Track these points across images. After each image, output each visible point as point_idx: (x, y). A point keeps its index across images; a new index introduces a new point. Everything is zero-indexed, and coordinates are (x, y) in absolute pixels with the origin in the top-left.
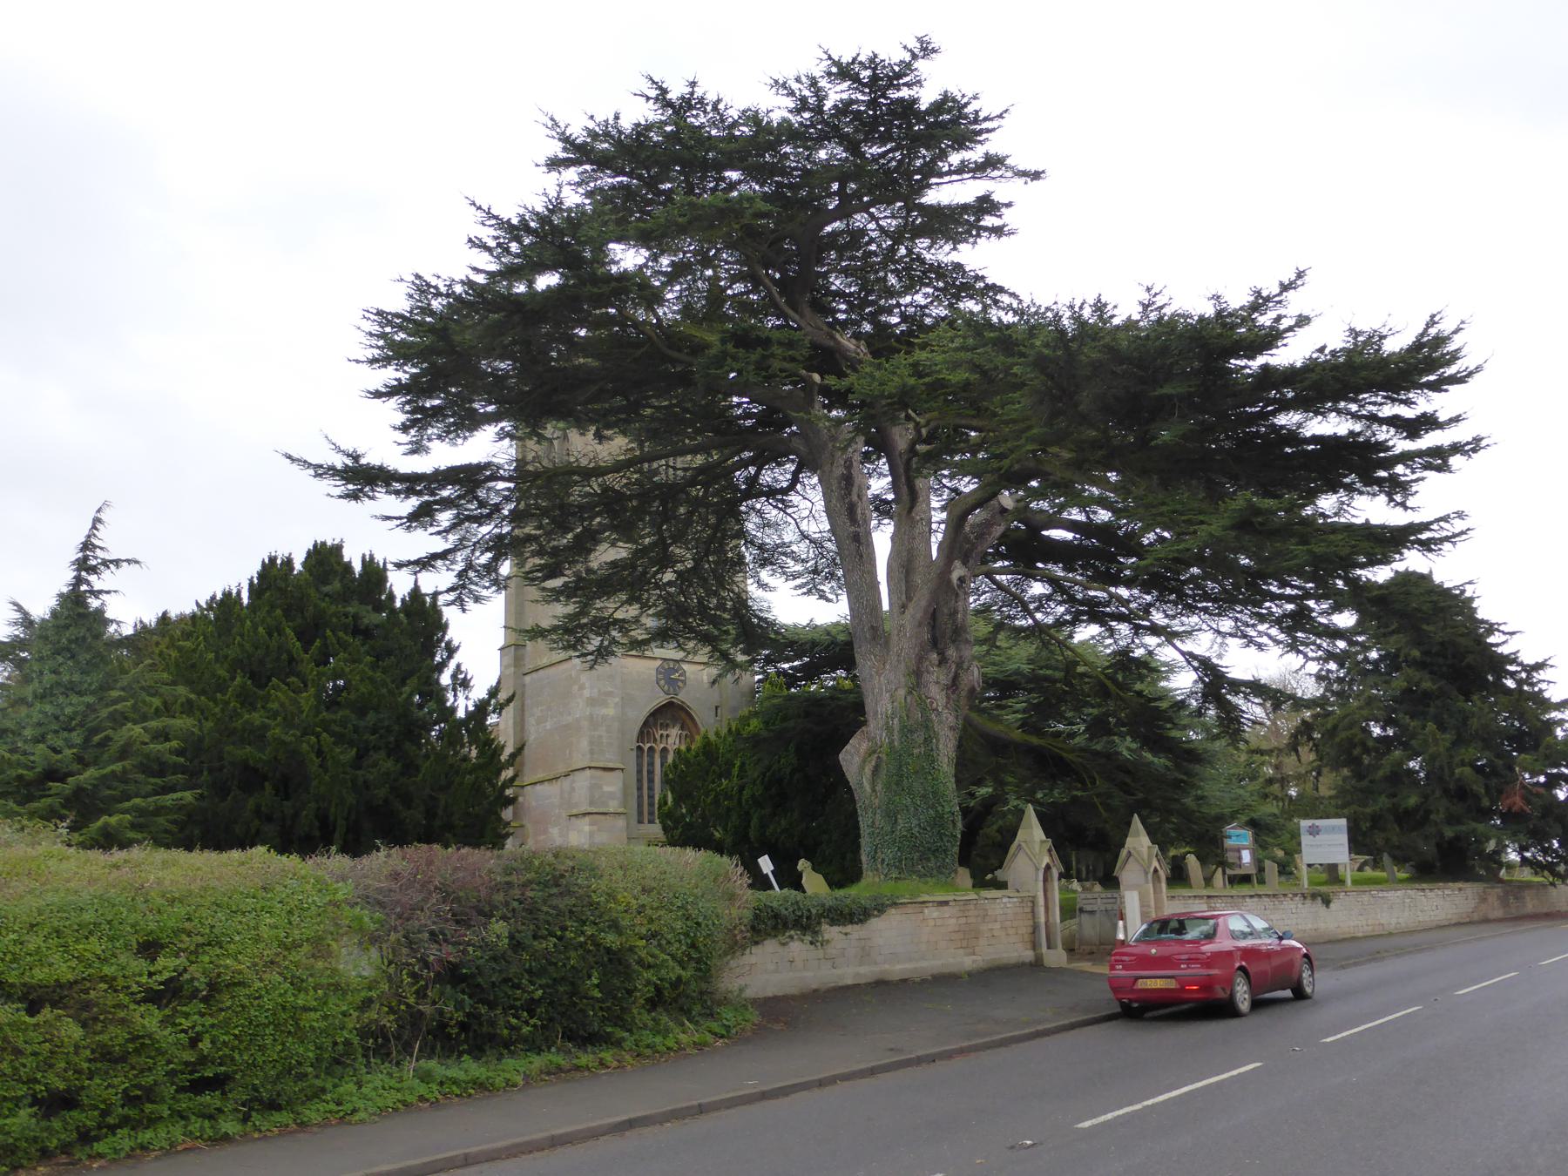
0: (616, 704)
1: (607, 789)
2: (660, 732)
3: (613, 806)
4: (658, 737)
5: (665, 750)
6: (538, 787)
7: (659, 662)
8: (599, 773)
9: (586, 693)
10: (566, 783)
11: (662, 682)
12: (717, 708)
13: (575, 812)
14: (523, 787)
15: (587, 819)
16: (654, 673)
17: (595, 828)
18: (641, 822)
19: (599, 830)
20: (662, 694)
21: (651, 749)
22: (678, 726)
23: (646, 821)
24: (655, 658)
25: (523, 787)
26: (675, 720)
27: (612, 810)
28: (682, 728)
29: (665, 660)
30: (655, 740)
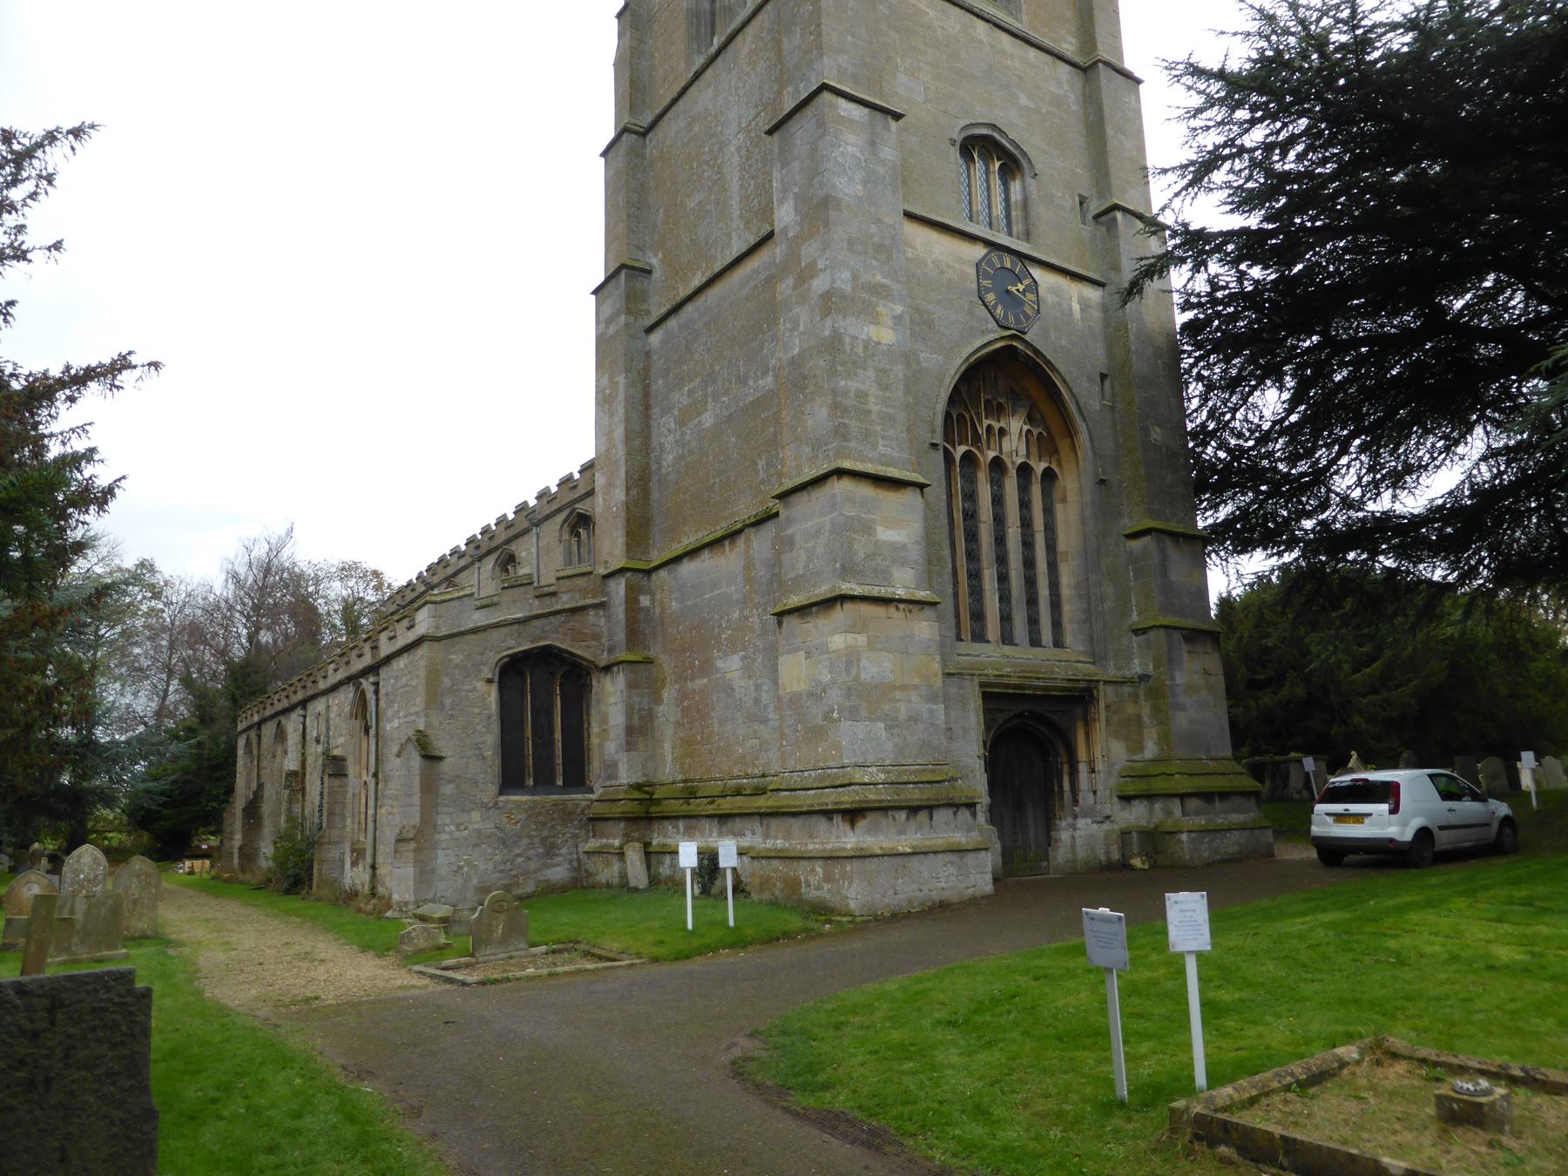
0: (898, 319)
1: (885, 535)
2: (986, 422)
3: (903, 583)
4: (982, 431)
5: (997, 465)
6: (687, 568)
7: (979, 251)
8: (865, 490)
9: (819, 284)
10: (760, 543)
11: (990, 297)
12: (1103, 377)
13: (795, 600)
14: (648, 572)
15: (840, 614)
17: (862, 639)
18: (959, 638)
19: (872, 646)
20: (992, 325)
21: (967, 456)
22: (1022, 413)
23: (966, 634)
25: (648, 572)
26: (1017, 399)
27: (901, 593)
28: (1030, 419)
30: (977, 439)
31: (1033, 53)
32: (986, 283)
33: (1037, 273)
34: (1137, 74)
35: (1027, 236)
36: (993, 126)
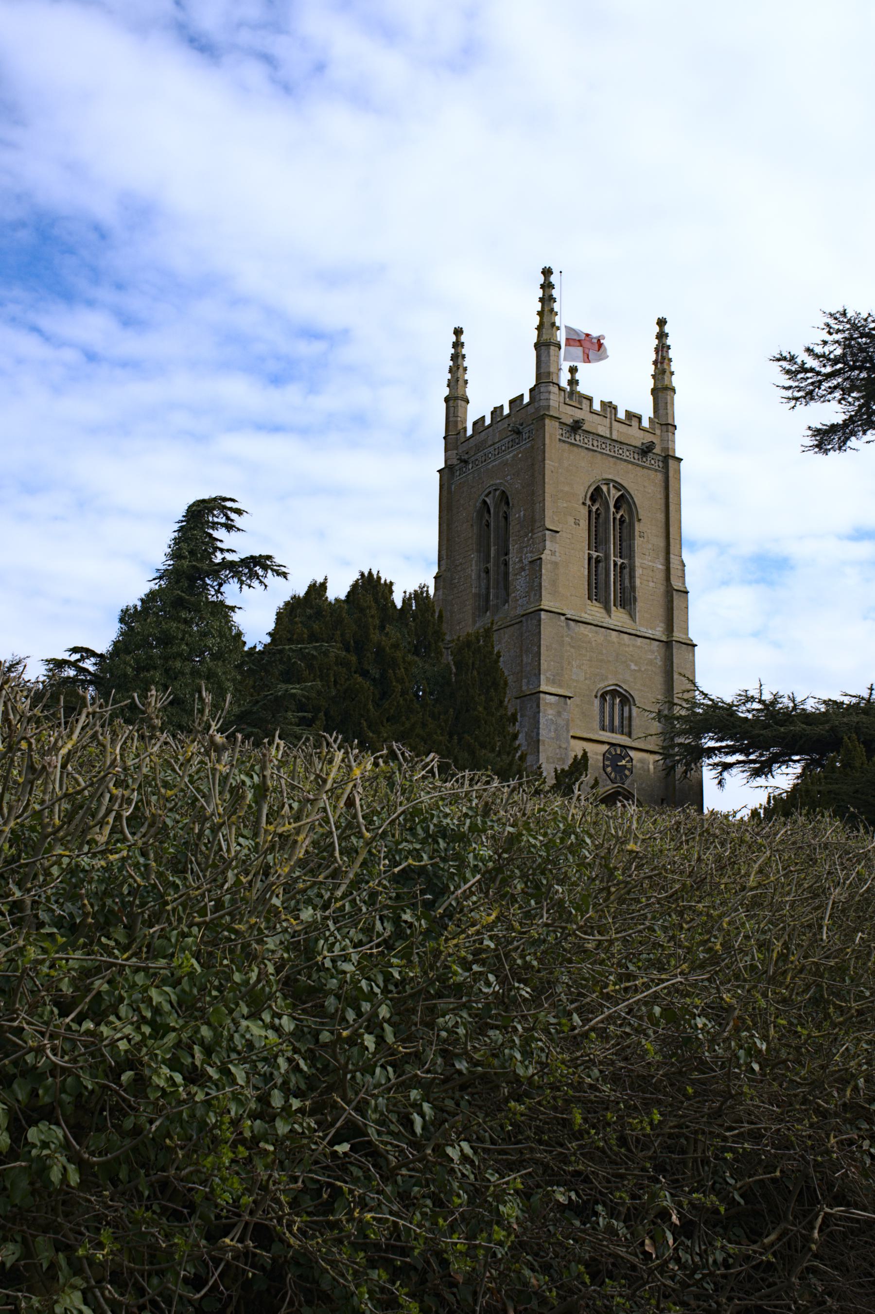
7: (606, 747)
11: (609, 769)
16: (601, 758)
20: (609, 782)
24: (603, 743)
29: (612, 745)
31: (640, 640)
32: (607, 763)
33: (632, 753)
34: (695, 642)
35: (629, 735)
36: (616, 685)
